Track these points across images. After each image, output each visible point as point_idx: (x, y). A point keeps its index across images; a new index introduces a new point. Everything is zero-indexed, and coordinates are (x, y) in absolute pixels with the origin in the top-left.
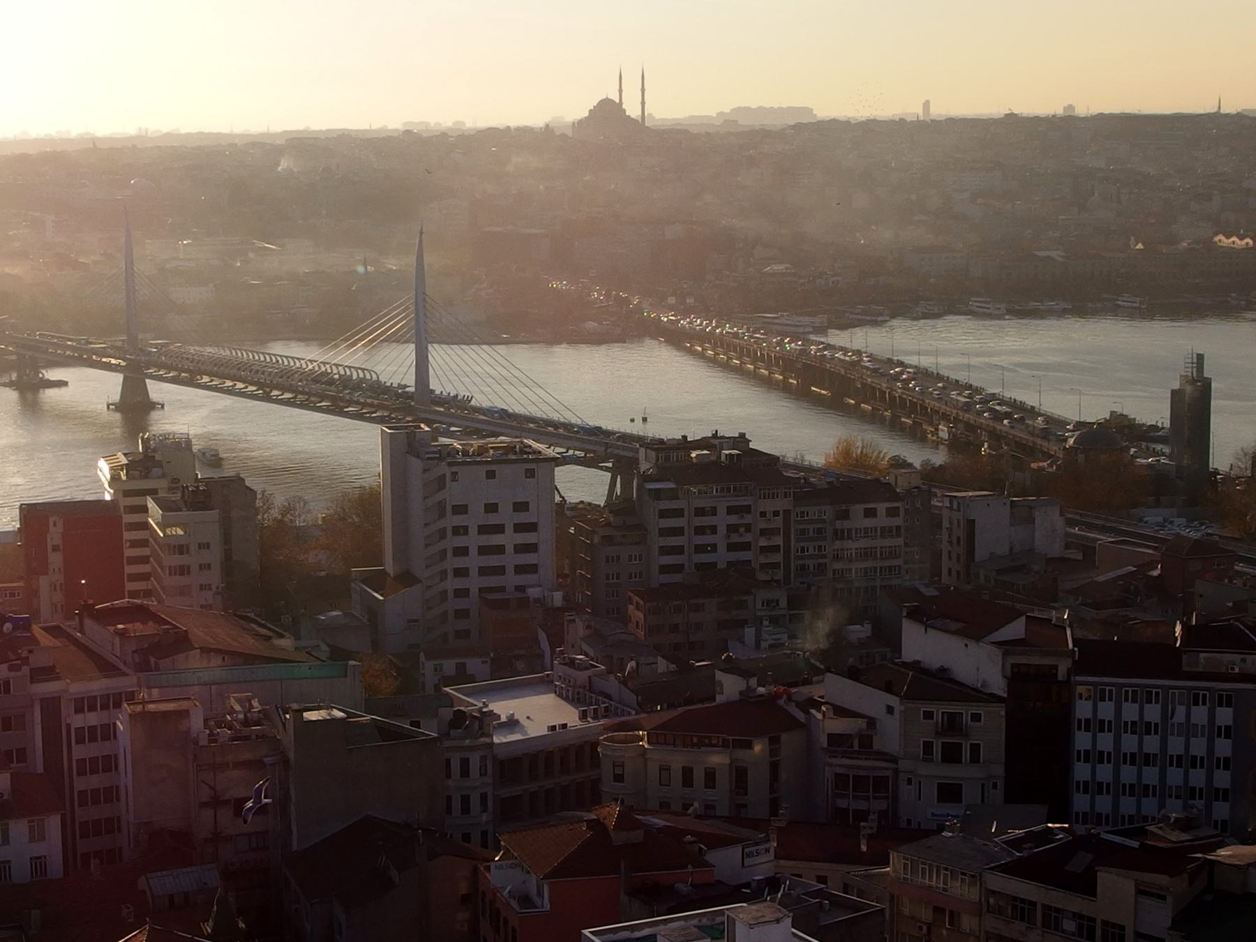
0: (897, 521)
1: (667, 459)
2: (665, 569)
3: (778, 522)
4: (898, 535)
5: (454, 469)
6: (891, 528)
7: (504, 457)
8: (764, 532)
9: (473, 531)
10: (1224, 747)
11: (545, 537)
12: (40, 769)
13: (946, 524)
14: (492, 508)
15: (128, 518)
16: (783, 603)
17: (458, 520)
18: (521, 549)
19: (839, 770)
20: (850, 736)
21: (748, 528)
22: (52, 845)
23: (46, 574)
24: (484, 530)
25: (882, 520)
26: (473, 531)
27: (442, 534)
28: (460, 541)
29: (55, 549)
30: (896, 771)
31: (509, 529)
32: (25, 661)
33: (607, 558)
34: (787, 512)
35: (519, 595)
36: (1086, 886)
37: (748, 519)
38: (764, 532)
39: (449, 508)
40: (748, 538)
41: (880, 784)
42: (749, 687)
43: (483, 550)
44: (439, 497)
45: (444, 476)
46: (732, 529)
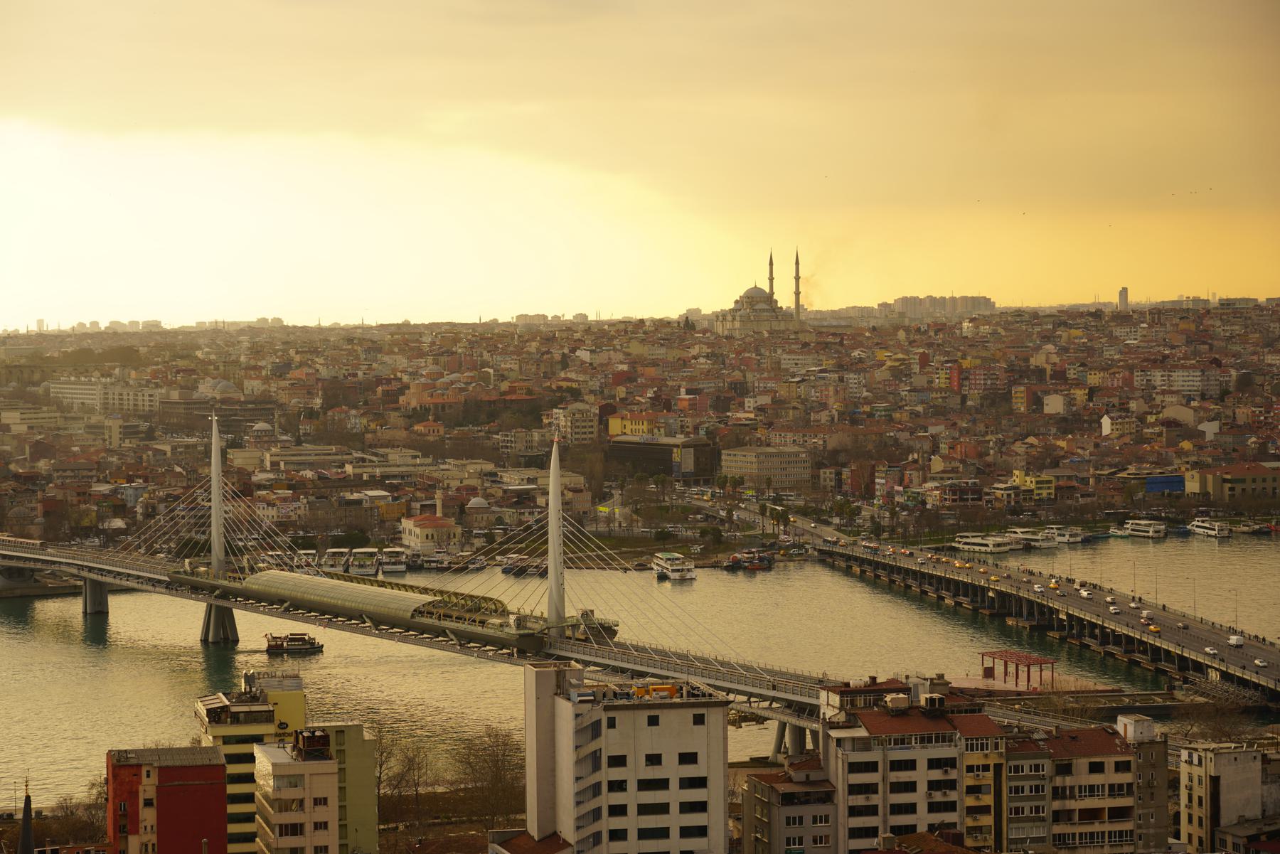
0: (1125, 778)
1: (853, 703)
2: (855, 833)
5: (611, 714)
6: (1120, 786)
7: (668, 701)
8: (973, 790)
9: (632, 786)
11: (714, 795)
13: (1184, 781)
14: (654, 760)
15: (233, 769)
17: (616, 774)
18: (688, 807)
21: (952, 785)
23: (136, 832)
24: (645, 785)
25: (1111, 777)
26: (632, 786)
27: (596, 790)
28: (617, 798)
29: (148, 803)
31: (674, 784)
33: (788, 818)
37: (953, 775)
38: (973, 790)
40: (953, 796)
43: (644, 809)
44: (593, 747)
45: (599, 722)
46: (933, 785)
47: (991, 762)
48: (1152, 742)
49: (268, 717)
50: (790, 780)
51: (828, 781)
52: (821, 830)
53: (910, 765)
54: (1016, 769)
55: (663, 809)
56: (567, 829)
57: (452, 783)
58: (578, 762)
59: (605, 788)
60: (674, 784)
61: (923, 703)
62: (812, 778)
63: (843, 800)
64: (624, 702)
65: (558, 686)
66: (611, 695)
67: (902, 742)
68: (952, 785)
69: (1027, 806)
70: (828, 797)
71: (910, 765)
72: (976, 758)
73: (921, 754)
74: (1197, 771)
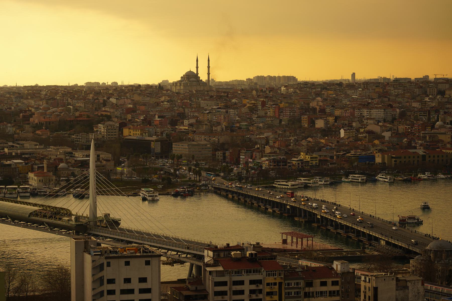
1: (219, 255)
4: (338, 295)
5: (108, 260)
6: (334, 292)
7: (134, 255)
9: (118, 292)
13: (362, 289)
14: (127, 281)
17: (111, 287)
21: (260, 291)
25: (330, 288)
26: (118, 292)
31: (137, 291)
37: (261, 287)
44: (100, 275)
45: (103, 263)
46: (252, 292)
47: (277, 281)
48: (349, 272)
50: (188, 289)
51: (205, 290)
53: (242, 283)
54: (288, 284)
57: (42, 291)
58: (94, 282)
59: (105, 293)
60: (137, 291)
61: (248, 255)
62: (198, 289)
64: (114, 255)
65: (85, 248)
66: (108, 252)
67: (238, 273)
68: (260, 291)
71: (242, 283)
72: (270, 280)
73: (246, 278)
74: (368, 285)
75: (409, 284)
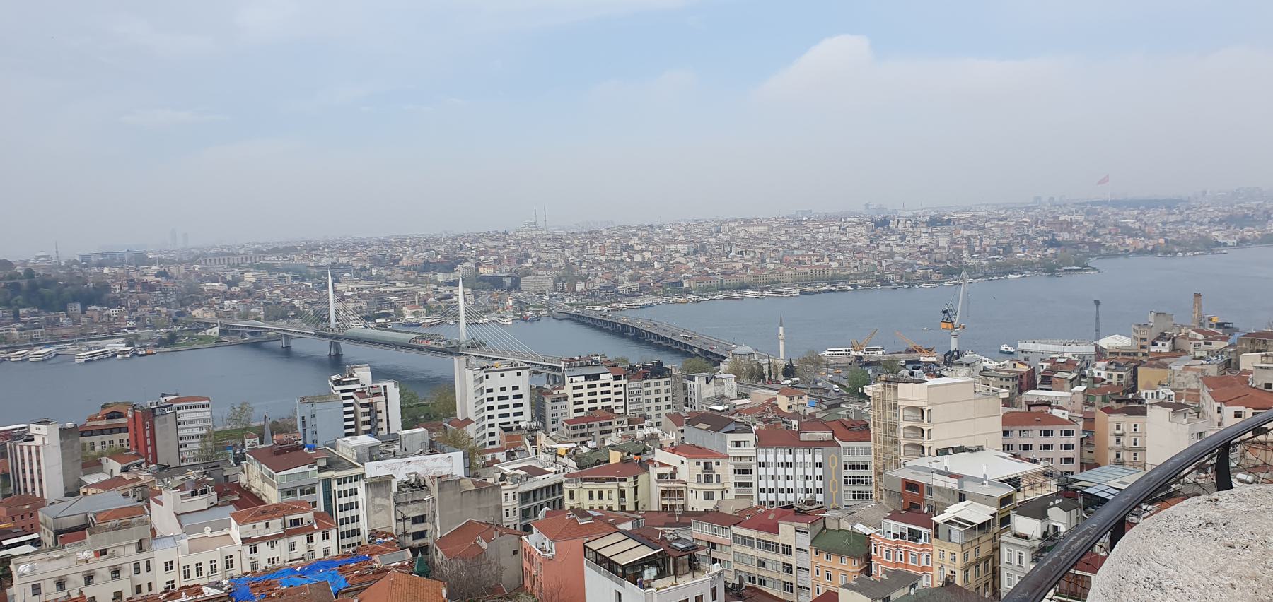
2: (576, 411)
3: (621, 389)
5: (487, 374)
9: (496, 399)
10: (819, 471)
12: (323, 510)
14: (503, 389)
16: (626, 422)
17: (490, 395)
18: (516, 406)
19: (662, 489)
20: (666, 474)
22: (332, 543)
24: (500, 398)
26: (496, 399)
30: (687, 488)
31: (511, 397)
32: (315, 463)
34: (625, 385)
35: (517, 425)
36: (775, 531)
39: (485, 391)
41: (680, 493)
42: (624, 456)
49: (357, 382)
52: (564, 410)
55: (507, 406)
56: (472, 417)
60: (511, 397)
63: (571, 400)
65: (467, 365)
69: (635, 398)
70: (566, 399)
75: (724, 381)
